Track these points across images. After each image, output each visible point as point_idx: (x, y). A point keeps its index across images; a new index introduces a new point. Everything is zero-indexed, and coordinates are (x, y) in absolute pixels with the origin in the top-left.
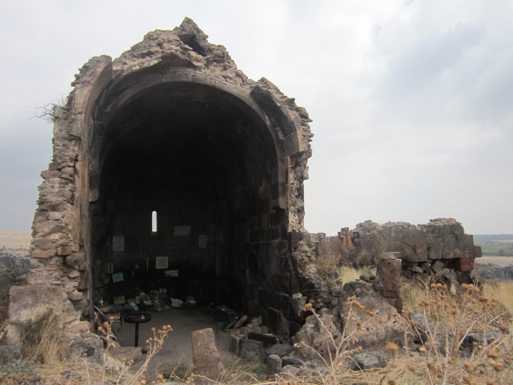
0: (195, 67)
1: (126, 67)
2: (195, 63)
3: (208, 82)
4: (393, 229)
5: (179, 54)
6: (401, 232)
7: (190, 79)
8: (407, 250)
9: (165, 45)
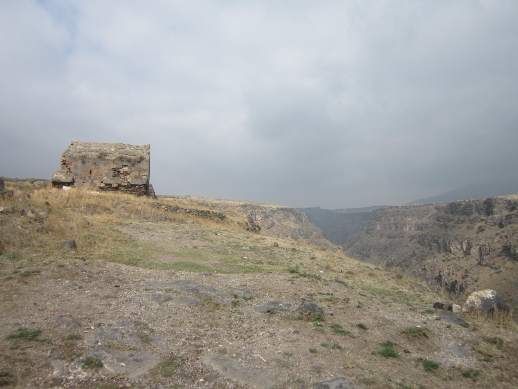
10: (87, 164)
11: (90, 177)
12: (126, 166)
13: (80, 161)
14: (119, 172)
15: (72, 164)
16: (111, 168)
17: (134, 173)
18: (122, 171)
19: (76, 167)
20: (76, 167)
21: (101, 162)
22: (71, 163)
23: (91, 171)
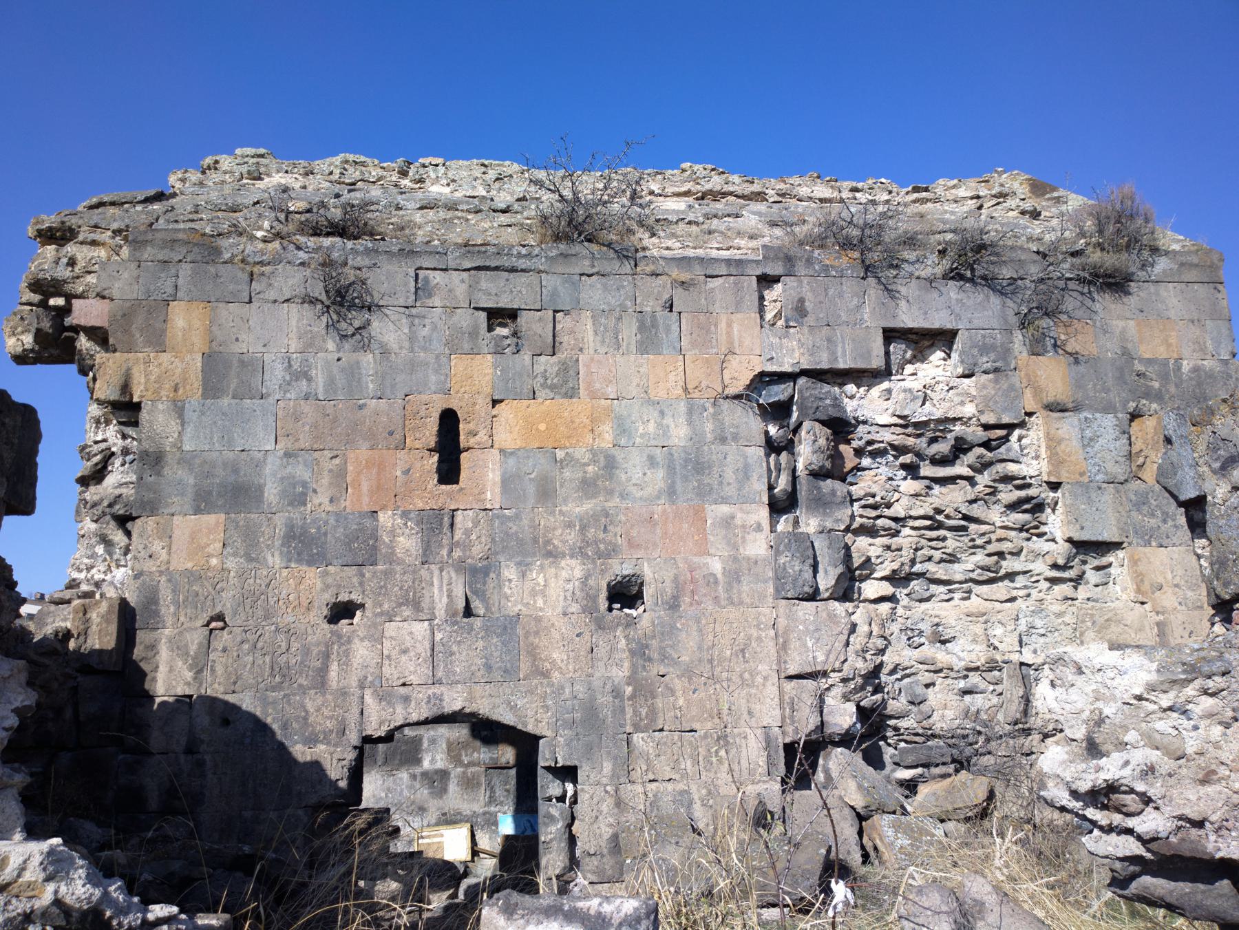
10: (388, 330)
11: (436, 524)
12: (926, 341)
13: (289, 280)
14: (840, 428)
16: (740, 375)
17: (1068, 427)
18: (872, 407)
19: (222, 373)
20: (222, 373)
21: (594, 292)
22: (143, 322)
23: (449, 420)
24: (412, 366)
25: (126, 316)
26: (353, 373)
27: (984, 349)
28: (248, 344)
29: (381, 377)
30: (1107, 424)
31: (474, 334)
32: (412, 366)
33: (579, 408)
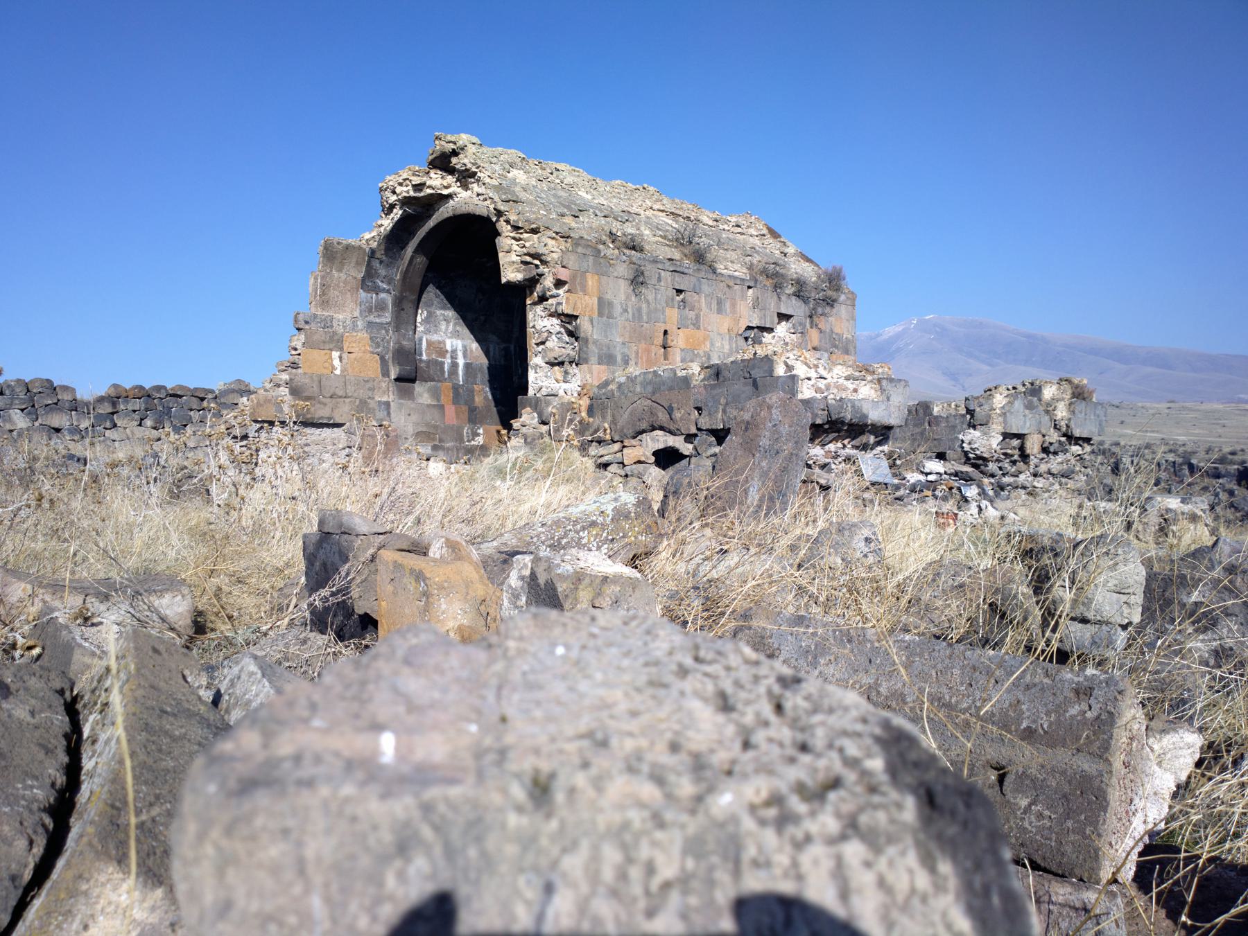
0: (450, 196)
1: (382, 229)
2: (445, 192)
3: (464, 210)
4: (639, 380)
5: (412, 193)
6: (650, 383)
7: (451, 214)
8: (660, 415)
9: (398, 190)
10: (648, 293)
12: (783, 317)
15: (584, 290)
19: (604, 306)
20: (604, 306)
23: (666, 332)
24: (656, 309)
25: (574, 277)
26: (639, 310)
27: (800, 324)
28: (609, 296)
29: (648, 314)
30: (826, 355)
31: (673, 299)
32: (656, 309)
33: (699, 334)
